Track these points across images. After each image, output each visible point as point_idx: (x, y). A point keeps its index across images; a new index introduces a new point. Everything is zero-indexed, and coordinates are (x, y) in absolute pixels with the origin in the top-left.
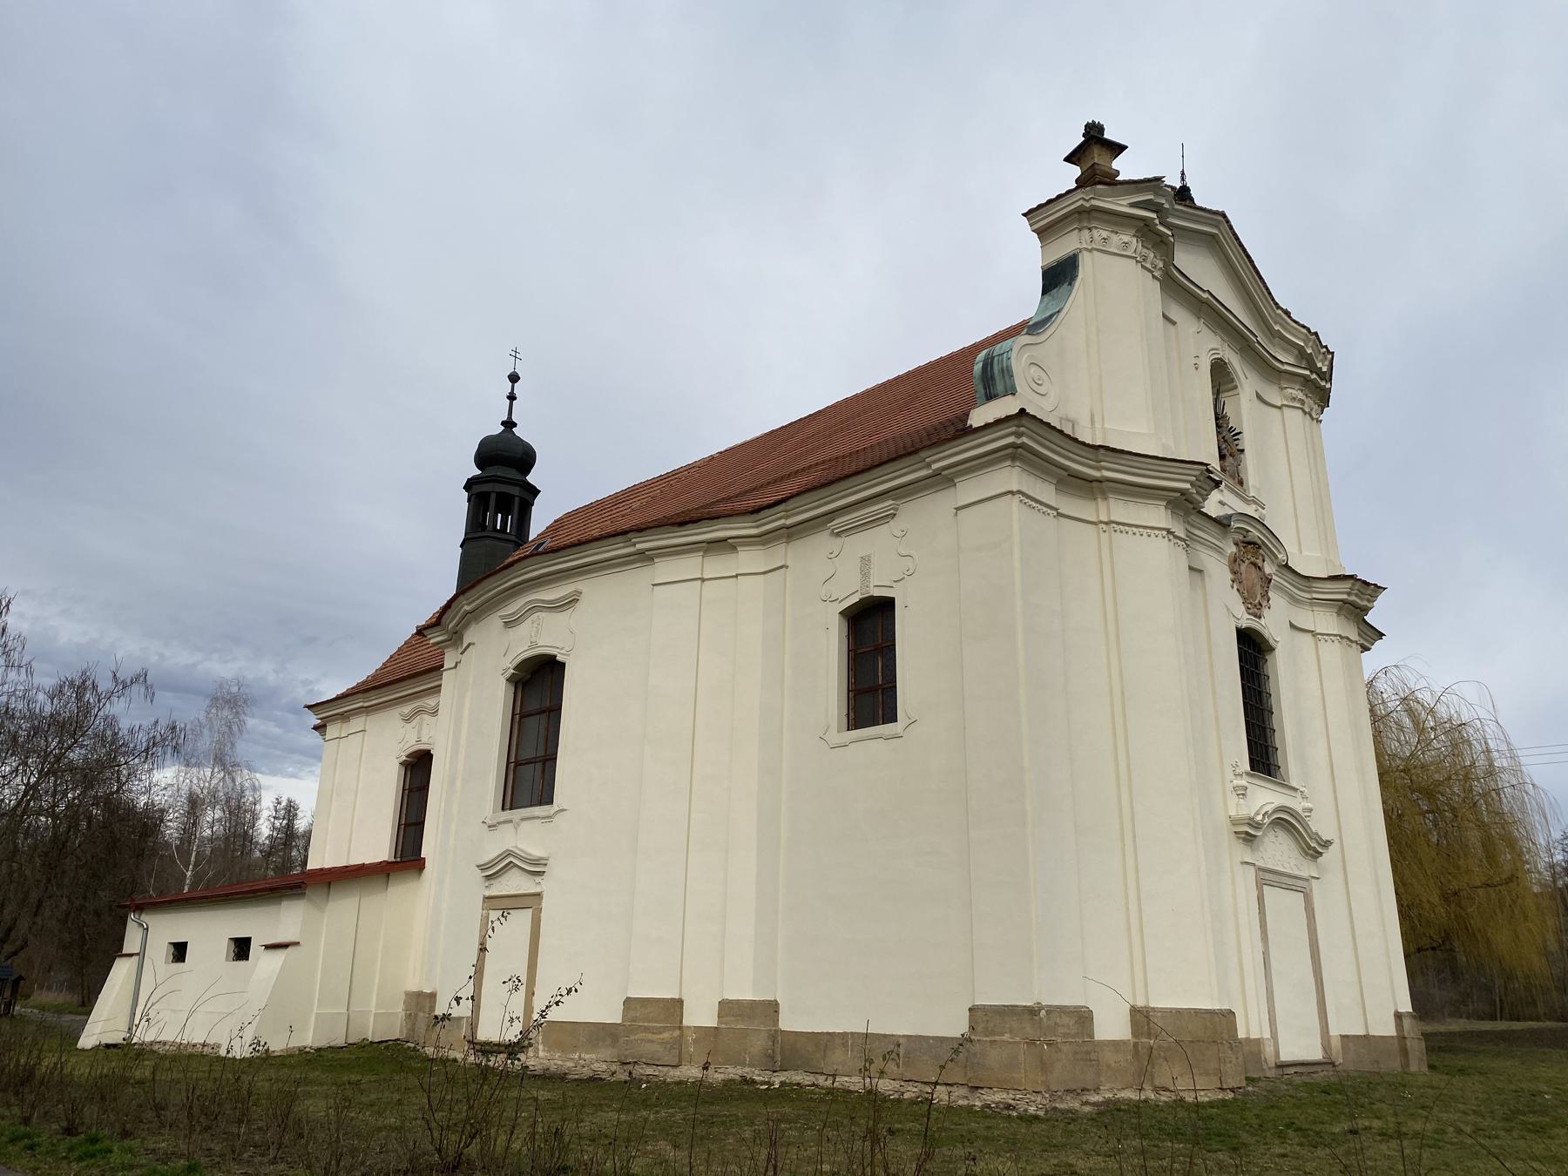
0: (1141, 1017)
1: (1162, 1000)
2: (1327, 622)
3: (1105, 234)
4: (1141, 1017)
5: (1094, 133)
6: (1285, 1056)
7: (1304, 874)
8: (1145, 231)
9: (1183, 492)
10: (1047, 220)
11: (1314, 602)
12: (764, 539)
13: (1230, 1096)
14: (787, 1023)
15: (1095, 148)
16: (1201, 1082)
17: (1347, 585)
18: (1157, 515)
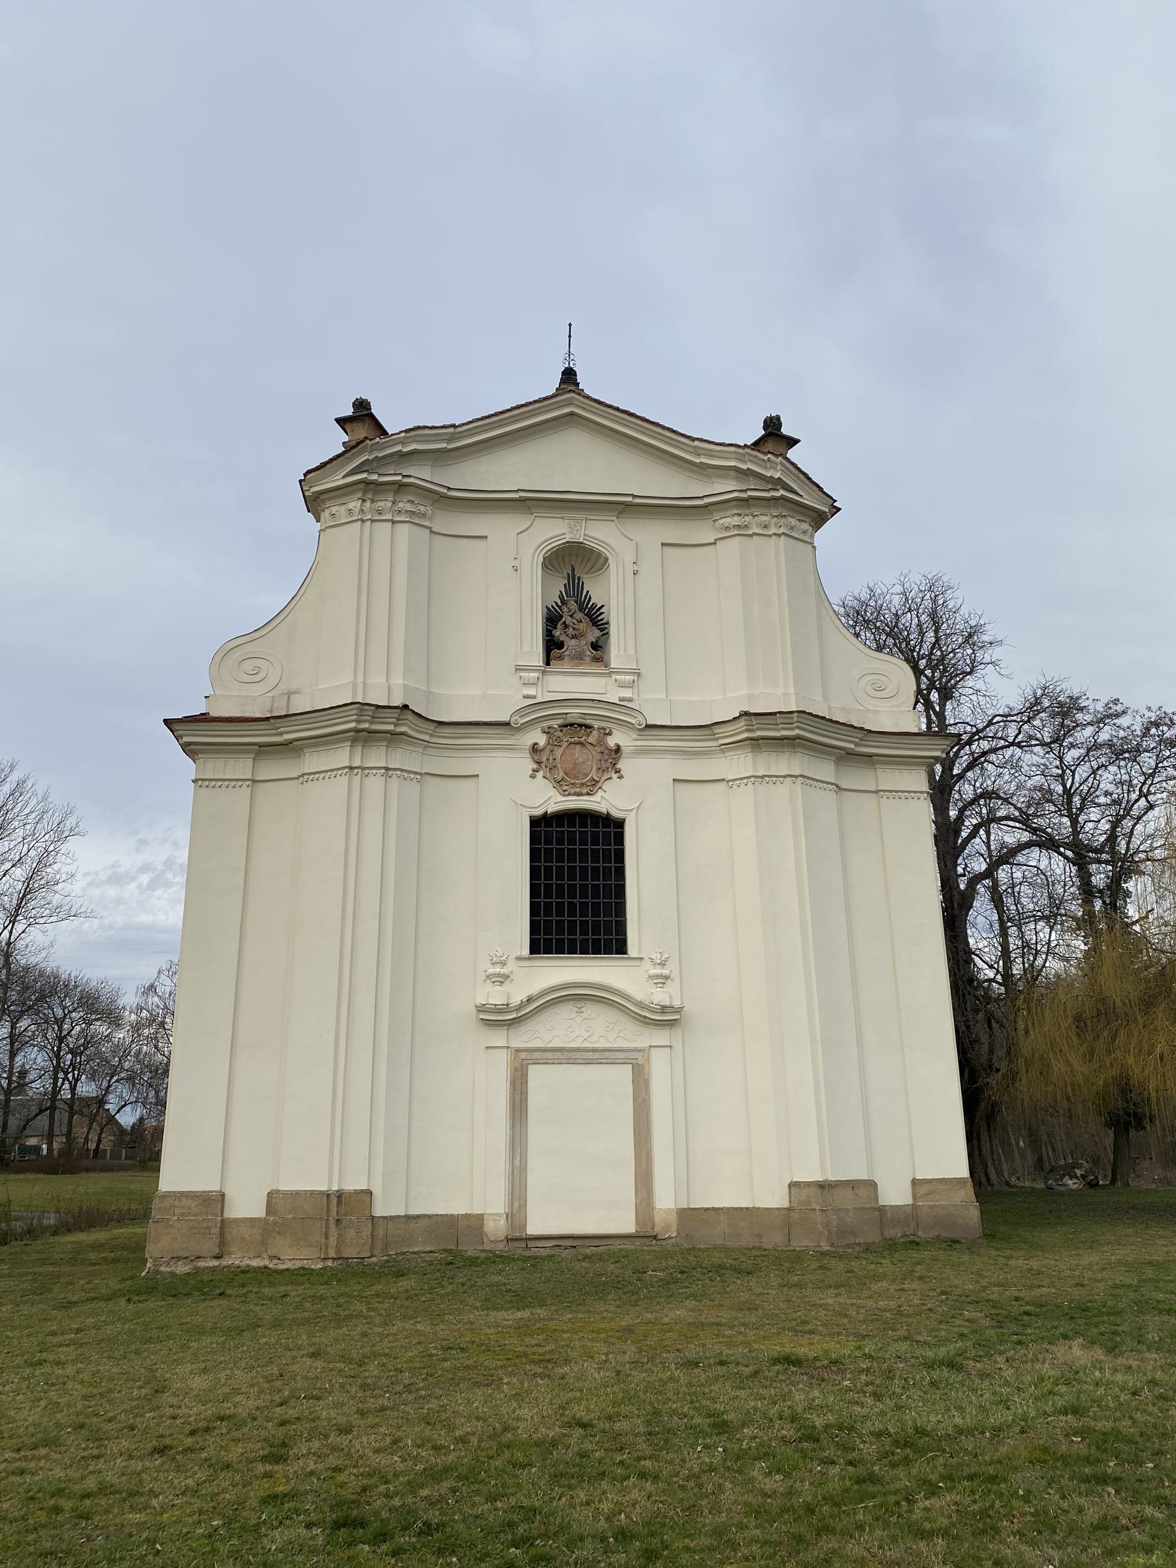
1: (288, 1184)
2: (741, 764)
7: (645, 1045)
16: (305, 1253)
17: (742, 723)
18: (341, 756)
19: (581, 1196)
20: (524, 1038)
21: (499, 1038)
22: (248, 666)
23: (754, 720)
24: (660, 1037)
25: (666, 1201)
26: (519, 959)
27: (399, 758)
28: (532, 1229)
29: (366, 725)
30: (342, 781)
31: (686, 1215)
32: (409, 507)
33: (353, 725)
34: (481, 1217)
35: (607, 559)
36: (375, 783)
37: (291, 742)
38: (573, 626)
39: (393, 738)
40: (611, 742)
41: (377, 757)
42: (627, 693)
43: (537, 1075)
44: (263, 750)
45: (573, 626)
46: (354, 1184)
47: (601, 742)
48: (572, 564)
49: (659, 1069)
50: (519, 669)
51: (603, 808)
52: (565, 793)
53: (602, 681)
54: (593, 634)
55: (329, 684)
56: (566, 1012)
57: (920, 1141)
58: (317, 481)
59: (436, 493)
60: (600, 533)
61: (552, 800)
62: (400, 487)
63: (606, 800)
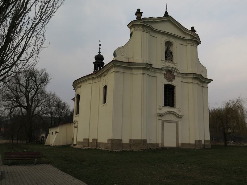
0: (130, 140)
2: (190, 81)
3: (136, 28)
4: (130, 140)
5: (139, 10)
6: (165, 146)
8: (144, 26)
9: (144, 67)
10: (131, 25)
11: (188, 78)
12: (98, 77)
13: (142, 150)
14: (99, 141)
15: (139, 13)
17: (193, 75)
18: (140, 71)
19: (170, 142)
20: (163, 118)
21: (160, 118)
22: (122, 52)
23: (195, 74)
24: (179, 120)
25: (180, 142)
26: (162, 106)
27: (149, 73)
28: (164, 146)
29: (146, 67)
30: (141, 75)
31: (182, 144)
32: (149, 30)
33: (144, 66)
34: (158, 144)
35: (173, 45)
36: (145, 76)
37: (131, 67)
38: (169, 55)
39: (148, 69)
40: (174, 74)
41: (146, 72)
42: (176, 67)
43: (165, 124)
44: (126, 68)
45: (169, 55)
46: (145, 138)
47: (173, 74)
48: (168, 44)
49: (180, 124)
50: (162, 60)
51: (173, 84)
52: (168, 81)
53: (172, 64)
54: (171, 57)
55: (138, 59)
56: (168, 115)
57: (205, 135)
58: (135, 22)
59: (152, 28)
60: (172, 40)
61: (166, 82)
62: (148, 27)
63: (174, 83)
